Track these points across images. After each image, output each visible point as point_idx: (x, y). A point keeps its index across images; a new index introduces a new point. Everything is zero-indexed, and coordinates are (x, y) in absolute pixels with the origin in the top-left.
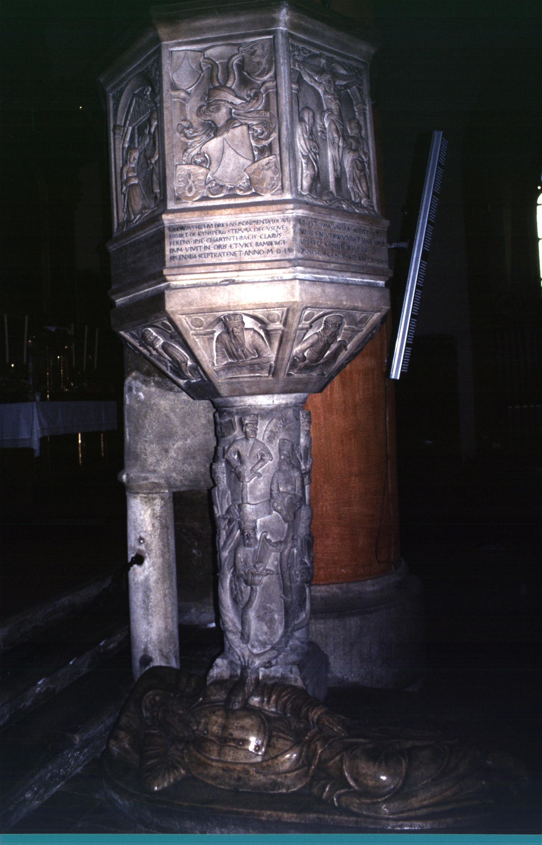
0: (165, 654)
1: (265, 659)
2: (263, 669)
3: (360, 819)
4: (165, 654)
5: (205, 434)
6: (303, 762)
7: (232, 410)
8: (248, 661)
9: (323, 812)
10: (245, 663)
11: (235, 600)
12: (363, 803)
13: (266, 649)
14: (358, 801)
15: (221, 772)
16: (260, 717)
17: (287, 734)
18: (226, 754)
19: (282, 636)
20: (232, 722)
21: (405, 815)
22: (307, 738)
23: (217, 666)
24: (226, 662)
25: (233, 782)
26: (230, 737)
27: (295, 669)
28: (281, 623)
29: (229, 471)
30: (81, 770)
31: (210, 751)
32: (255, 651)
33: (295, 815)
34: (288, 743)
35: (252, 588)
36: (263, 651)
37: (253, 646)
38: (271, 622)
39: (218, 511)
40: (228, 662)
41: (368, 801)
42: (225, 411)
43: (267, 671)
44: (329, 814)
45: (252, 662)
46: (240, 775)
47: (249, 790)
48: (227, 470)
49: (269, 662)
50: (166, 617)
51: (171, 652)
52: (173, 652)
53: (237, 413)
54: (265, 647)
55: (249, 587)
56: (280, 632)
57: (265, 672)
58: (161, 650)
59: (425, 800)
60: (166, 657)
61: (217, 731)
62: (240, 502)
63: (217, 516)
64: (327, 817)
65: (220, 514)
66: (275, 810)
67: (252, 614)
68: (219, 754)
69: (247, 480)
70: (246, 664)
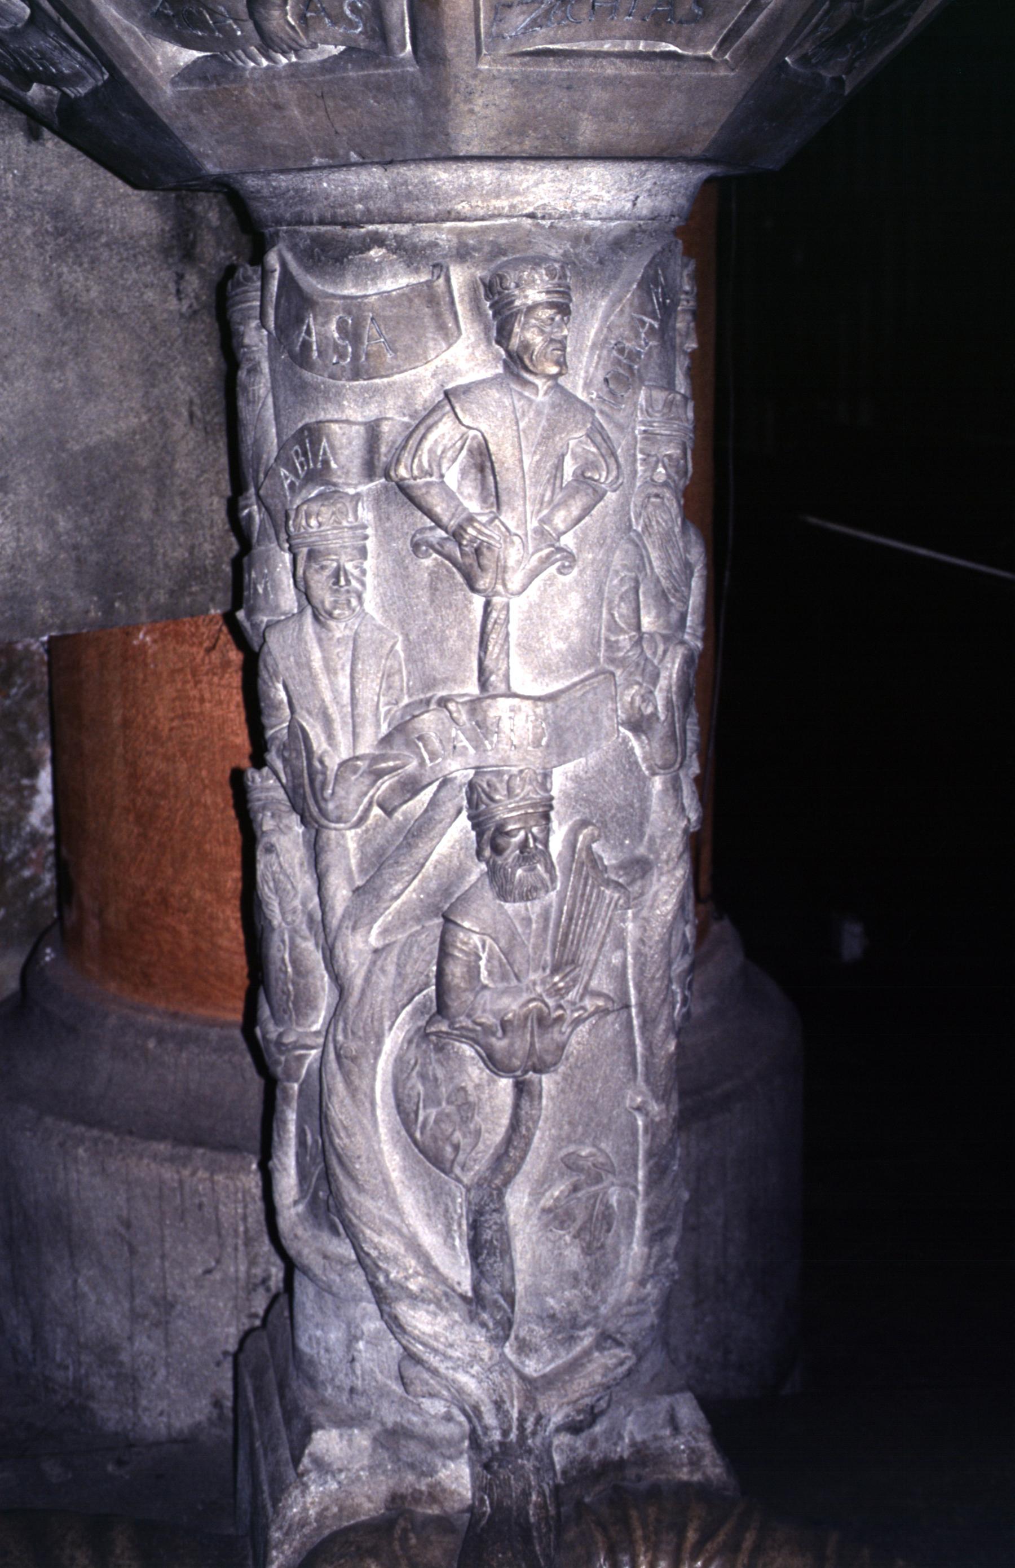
5: (47, 365)
7: (427, 233)
8: (522, 1420)
10: (505, 1433)
11: (431, 1155)
13: (577, 1350)
23: (321, 1465)
24: (362, 1439)
29: (403, 545)
32: (532, 1367)
35: (521, 1088)
37: (524, 1347)
39: (330, 737)
40: (375, 1439)
42: (378, 240)
43: (580, 1443)
45: (539, 1418)
48: (386, 536)
53: (462, 254)
54: (571, 1340)
55: (505, 1084)
57: (573, 1449)
62: (473, 689)
63: (333, 763)
65: (345, 754)
69: (515, 580)
70: (513, 1436)
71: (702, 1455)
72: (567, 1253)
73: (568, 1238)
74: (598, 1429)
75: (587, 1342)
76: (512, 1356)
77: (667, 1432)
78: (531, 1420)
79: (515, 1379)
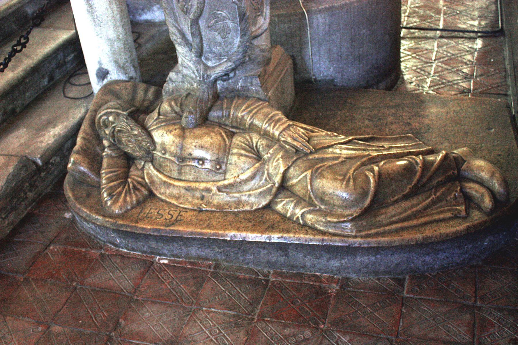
0: (122, 65)
1: (220, 70)
2: (222, 82)
3: (326, 238)
4: (122, 65)
6: (266, 179)
8: (203, 75)
9: (288, 231)
10: (200, 78)
12: (329, 222)
13: (222, 61)
14: (324, 220)
15: (183, 191)
16: (221, 134)
17: (250, 152)
18: (187, 173)
19: (239, 47)
20: (190, 141)
21: (373, 231)
22: (269, 155)
23: (170, 79)
24: (180, 76)
25: (196, 201)
26: (189, 157)
27: (256, 81)
28: (236, 31)
30: (51, 189)
31: (171, 171)
32: (210, 64)
33: (259, 235)
34: (250, 160)
36: (218, 64)
37: (207, 59)
38: (225, 32)
41: (335, 220)
44: (295, 233)
45: (208, 76)
46: (203, 193)
47: (213, 209)
49: (227, 74)
50: (115, 27)
51: (127, 62)
52: (129, 61)
54: (220, 59)
56: (237, 41)
57: (223, 85)
58: (116, 62)
59: (394, 216)
60: (122, 68)
61: (175, 151)
64: (292, 235)
66: (238, 229)
67: (202, 23)
68: (180, 173)
71: (259, 91)
72: (217, 37)
73: (217, 34)
74: (230, 81)
75: (225, 60)
76: (204, 61)
77: (249, 85)
78: (206, 76)
79: (202, 66)
